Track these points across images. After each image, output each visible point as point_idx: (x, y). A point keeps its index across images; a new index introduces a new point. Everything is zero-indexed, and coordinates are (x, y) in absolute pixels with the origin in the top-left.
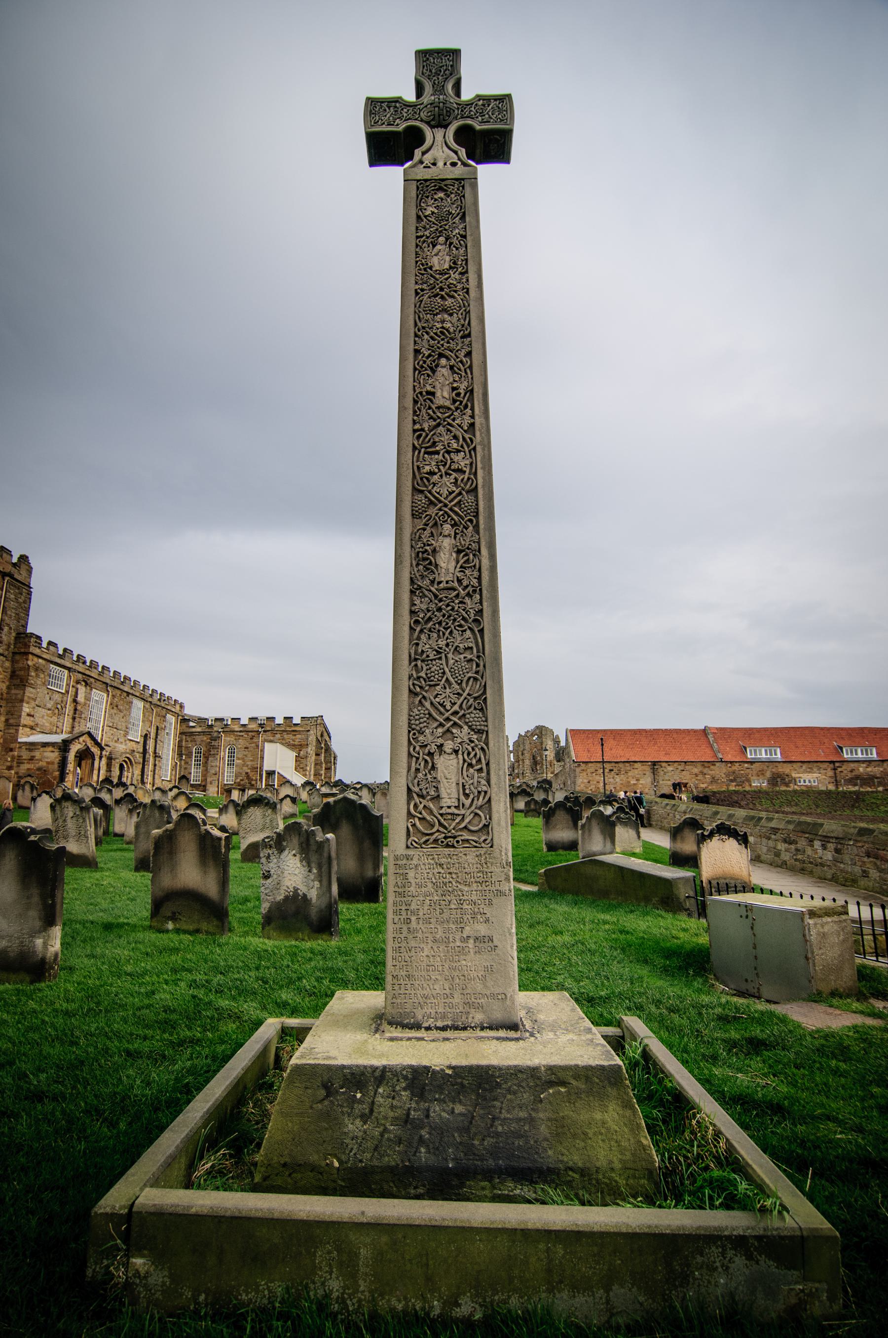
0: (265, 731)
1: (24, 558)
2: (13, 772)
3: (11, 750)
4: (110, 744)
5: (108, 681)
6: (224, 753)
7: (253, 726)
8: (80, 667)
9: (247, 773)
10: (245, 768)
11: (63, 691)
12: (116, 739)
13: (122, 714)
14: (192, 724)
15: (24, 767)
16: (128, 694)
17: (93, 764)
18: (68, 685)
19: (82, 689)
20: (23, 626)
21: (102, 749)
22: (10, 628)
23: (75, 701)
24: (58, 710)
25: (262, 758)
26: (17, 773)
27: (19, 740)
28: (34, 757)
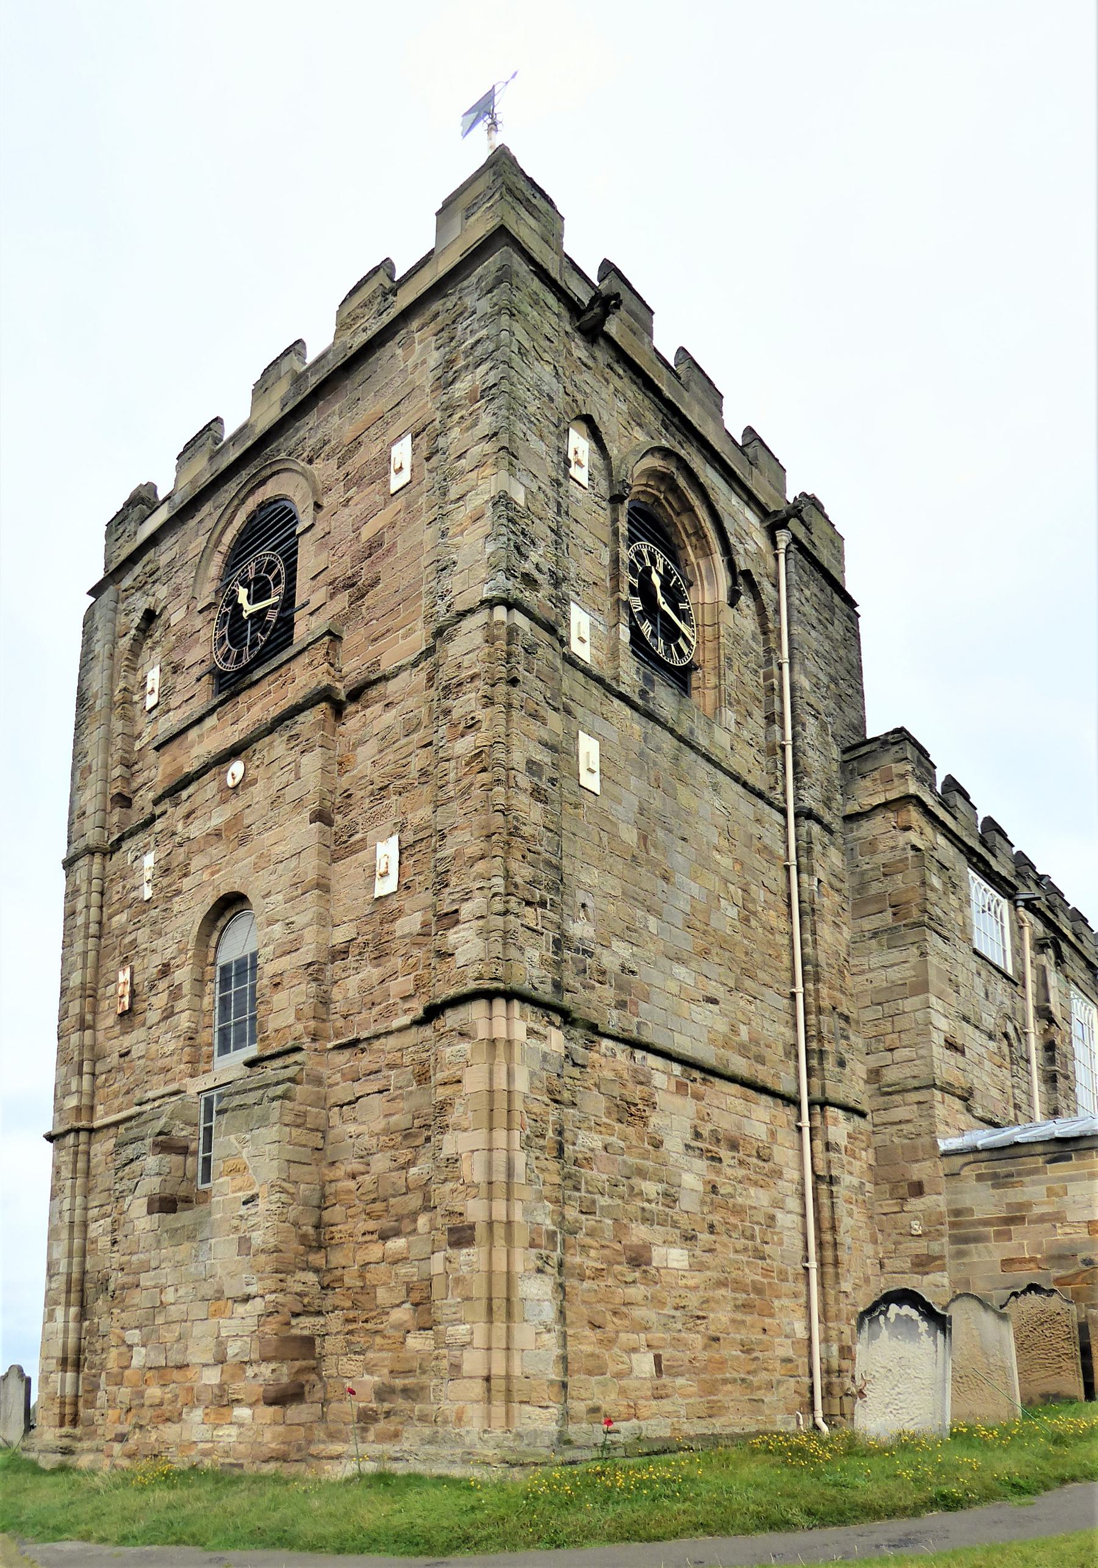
3: (918, 1189)
27: (943, 1145)
28: (1027, 1206)
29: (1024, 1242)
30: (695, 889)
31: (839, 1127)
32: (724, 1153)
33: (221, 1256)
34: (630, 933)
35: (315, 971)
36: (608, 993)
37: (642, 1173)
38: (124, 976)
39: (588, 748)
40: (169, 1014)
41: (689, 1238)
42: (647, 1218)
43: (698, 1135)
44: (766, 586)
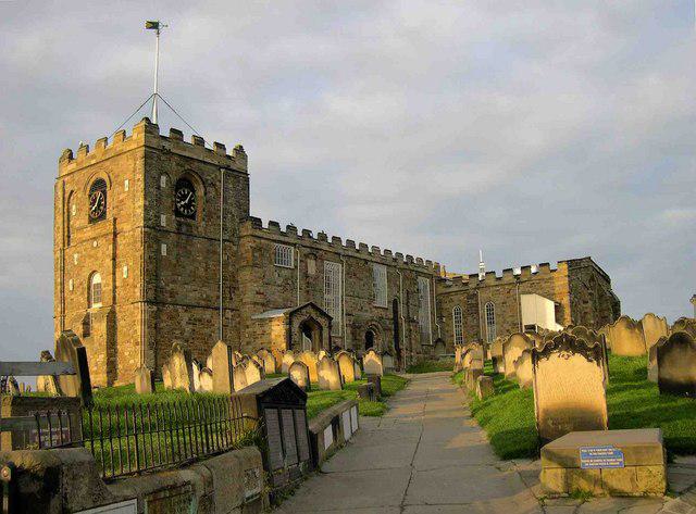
1: (240, 150)
2: (250, 347)
5: (341, 251)
6: (483, 311)
7: (509, 278)
8: (307, 242)
11: (292, 267)
14: (448, 283)
16: (366, 261)
17: (321, 335)
18: (296, 260)
19: (312, 266)
21: (330, 319)
23: (306, 276)
24: (288, 285)
25: (520, 311)
31: (229, 314)
33: (96, 345)
34: (174, 282)
38: (71, 282)
39: (164, 247)
40: (83, 293)
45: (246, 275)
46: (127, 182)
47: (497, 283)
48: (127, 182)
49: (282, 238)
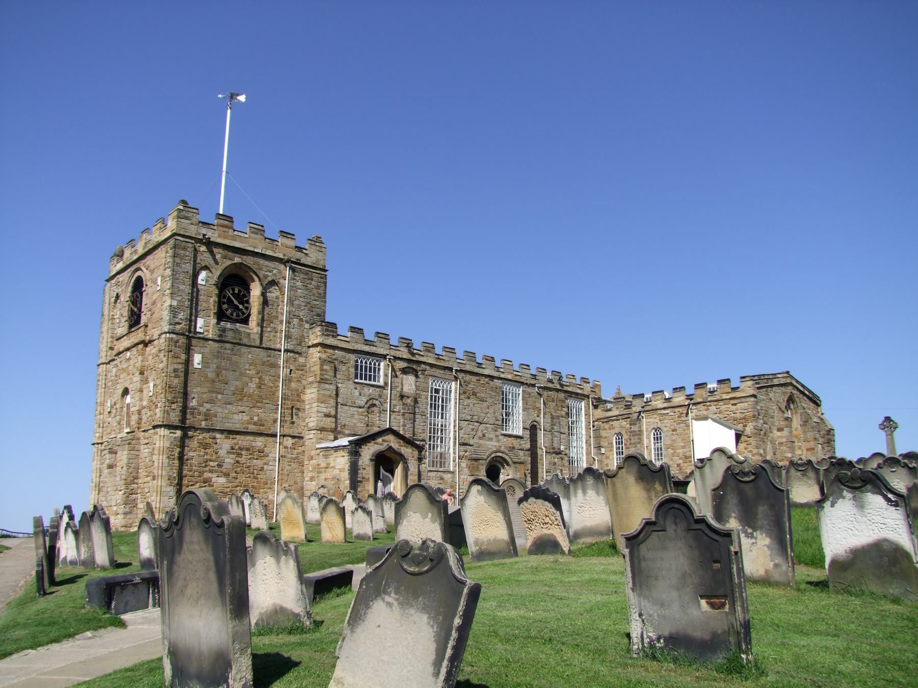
0: (694, 404)
2: (313, 483)
4: (471, 442)
9: (678, 465)
10: (676, 458)
11: (382, 383)
12: (480, 434)
13: (485, 404)
14: (609, 406)
15: (323, 476)
16: (492, 378)
18: (386, 375)
20: (318, 315)
22: (301, 320)
26: (317, 484)
29: (329, 474)
30: (237, 383)
31: (289, 442)
32: (244, 452)
35: (139, 412)
36: (201, 417)
37: (211, 461)
41: (227, 475)
42: (211, 471)
43: (232, 449)
44: (281, 281)
45: (311, 394)
46: (159, 279)
47: (665, 405)
48: (159, 279)
49: (367, 348)
